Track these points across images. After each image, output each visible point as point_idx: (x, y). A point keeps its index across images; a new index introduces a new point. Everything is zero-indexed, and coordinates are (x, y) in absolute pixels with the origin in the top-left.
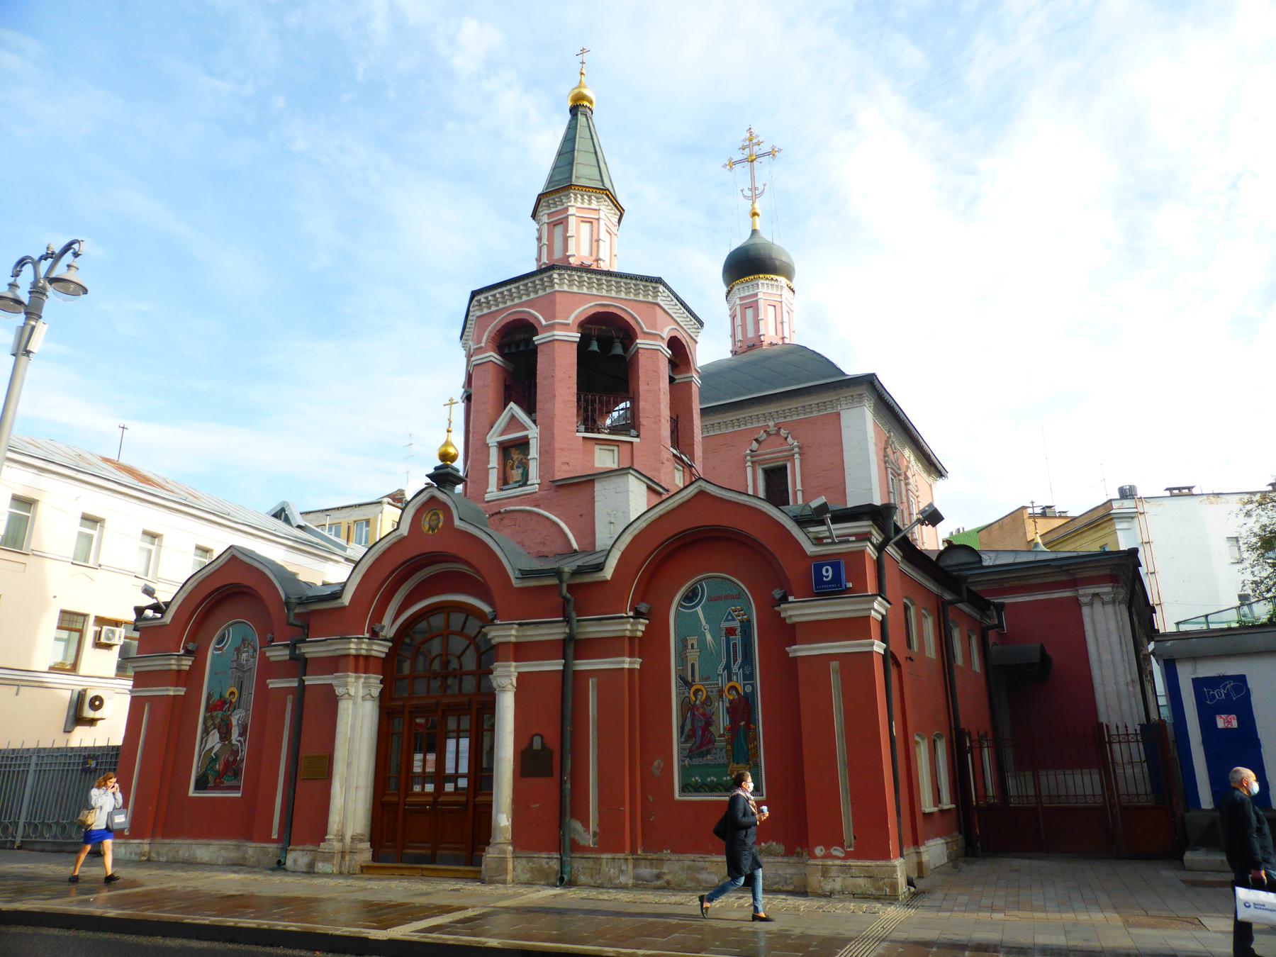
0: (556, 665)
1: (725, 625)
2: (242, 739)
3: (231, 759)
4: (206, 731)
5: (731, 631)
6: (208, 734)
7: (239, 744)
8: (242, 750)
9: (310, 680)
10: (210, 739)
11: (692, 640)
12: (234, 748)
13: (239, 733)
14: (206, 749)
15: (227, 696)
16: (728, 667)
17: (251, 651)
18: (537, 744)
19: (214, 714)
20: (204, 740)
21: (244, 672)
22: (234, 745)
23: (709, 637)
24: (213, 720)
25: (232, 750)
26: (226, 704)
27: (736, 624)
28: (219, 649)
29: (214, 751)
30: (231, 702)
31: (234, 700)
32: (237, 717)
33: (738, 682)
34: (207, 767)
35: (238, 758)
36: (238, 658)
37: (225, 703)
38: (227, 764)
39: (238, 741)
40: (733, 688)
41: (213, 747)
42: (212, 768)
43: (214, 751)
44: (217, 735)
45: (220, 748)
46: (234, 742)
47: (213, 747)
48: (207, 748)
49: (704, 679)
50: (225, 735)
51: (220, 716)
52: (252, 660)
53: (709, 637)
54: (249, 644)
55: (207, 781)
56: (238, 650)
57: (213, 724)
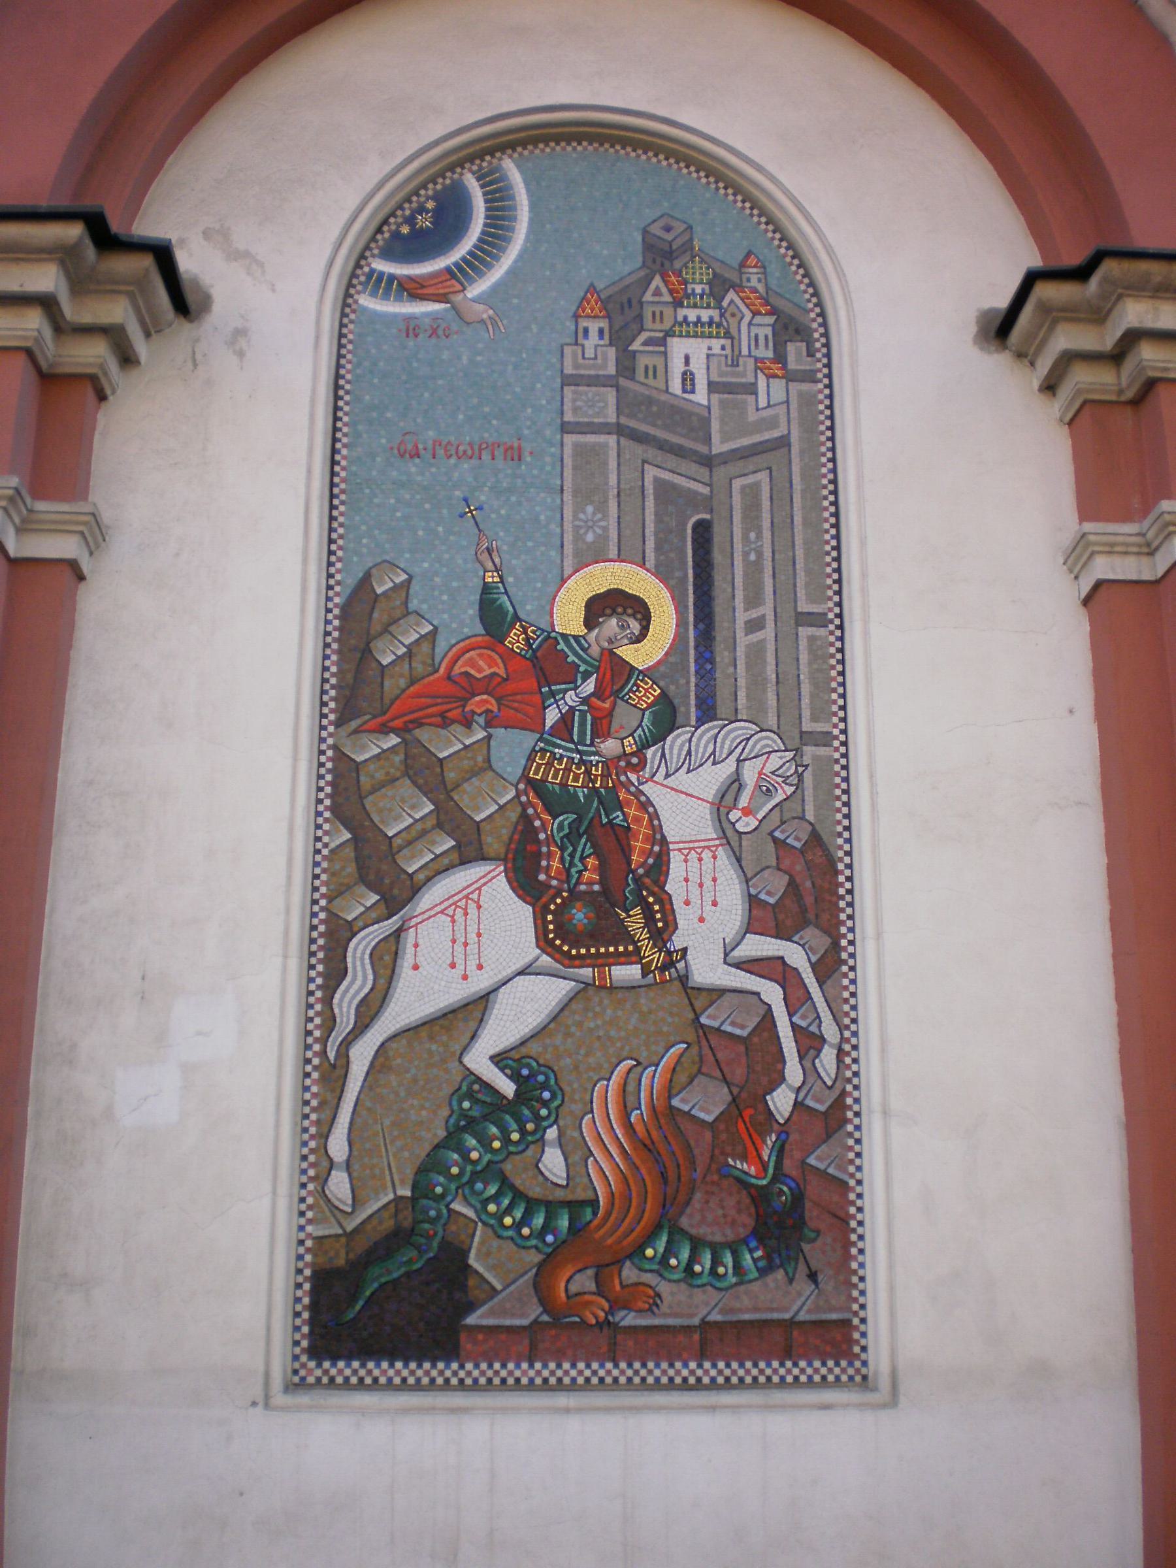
2: (795, 955)
7: (772, 994)
8: (809, 1043)
13: (753, 901)
20: (359, 949)
21: (708, 462)
22: (717, 993)
26: (571, 676)
28: (413, 289)
31: (641, 656)
32: (710, 780)
34: (431, 1165)
35: (781, 1102)
36: (627, 365)
39: (750, 966)
41: (482, 1003)
42: (491, 1171)
45: (555, 1021)
47: (482, 1003)
52: (769, 391)
54: (719, 286)
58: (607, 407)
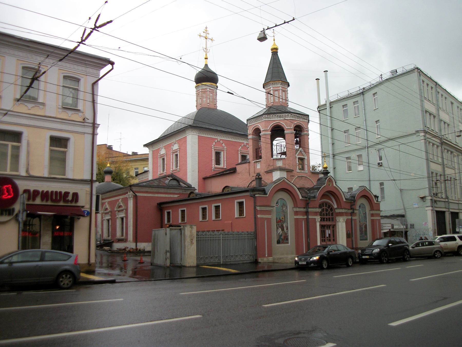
0: (350, 217)
1: (364, 212)
2: (287, 230)
3: (285, 235)
4: (277, 228)
5: (364, 214)
6: (278, 229)
9: (310, 217)
10: (279, 230)
11: (360, 215)
12: (286, 233)
14: (278, 233)
15: (281, 219)
16: (364, 220)
17: (286, 207)
18: (348, 233)
19: (279, 223)
23: (362, 214)
24: (279, 225)
25: (285, 233)
27: (365, 212)
29: (280, 233)
30: (283, 221)
31: (283, 220)
32: (285, 225)
33: (365, 222)
37: (281, 221)
38: (284, 237)
40: (365, 223)
41: (280, 232)
43: (280, 233)
44: (281, 229)
46: (285, 231)
47: (280, 232)
48: (278, 233)
49: (362, 221)
50: (283, 229)
51: (280, 224)
52: (286, 210)
53: (362, 214)
55: (280, 241)
56: (282, 206)
57: (279, 226)
58: (282, 210)
